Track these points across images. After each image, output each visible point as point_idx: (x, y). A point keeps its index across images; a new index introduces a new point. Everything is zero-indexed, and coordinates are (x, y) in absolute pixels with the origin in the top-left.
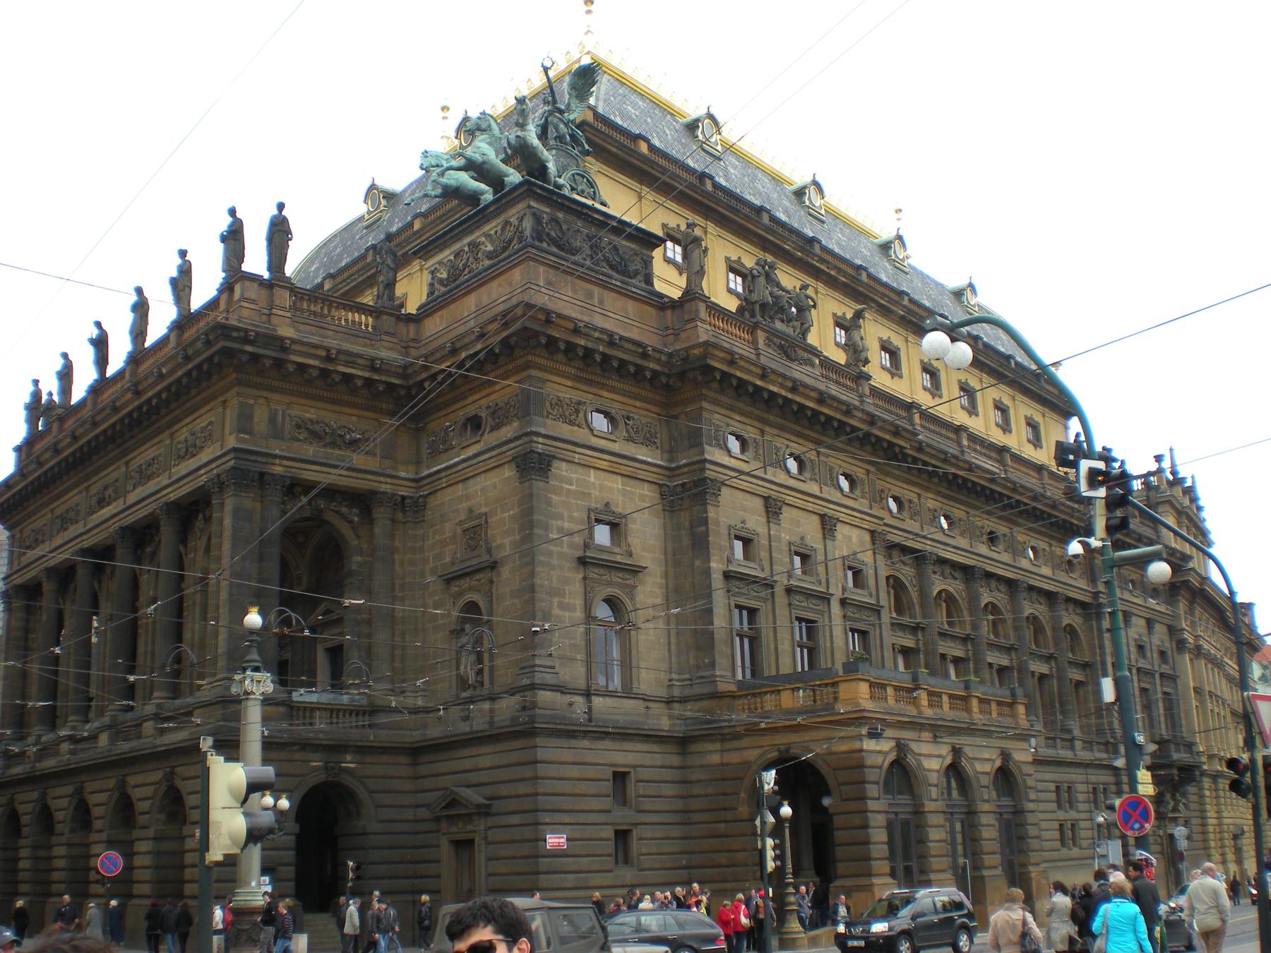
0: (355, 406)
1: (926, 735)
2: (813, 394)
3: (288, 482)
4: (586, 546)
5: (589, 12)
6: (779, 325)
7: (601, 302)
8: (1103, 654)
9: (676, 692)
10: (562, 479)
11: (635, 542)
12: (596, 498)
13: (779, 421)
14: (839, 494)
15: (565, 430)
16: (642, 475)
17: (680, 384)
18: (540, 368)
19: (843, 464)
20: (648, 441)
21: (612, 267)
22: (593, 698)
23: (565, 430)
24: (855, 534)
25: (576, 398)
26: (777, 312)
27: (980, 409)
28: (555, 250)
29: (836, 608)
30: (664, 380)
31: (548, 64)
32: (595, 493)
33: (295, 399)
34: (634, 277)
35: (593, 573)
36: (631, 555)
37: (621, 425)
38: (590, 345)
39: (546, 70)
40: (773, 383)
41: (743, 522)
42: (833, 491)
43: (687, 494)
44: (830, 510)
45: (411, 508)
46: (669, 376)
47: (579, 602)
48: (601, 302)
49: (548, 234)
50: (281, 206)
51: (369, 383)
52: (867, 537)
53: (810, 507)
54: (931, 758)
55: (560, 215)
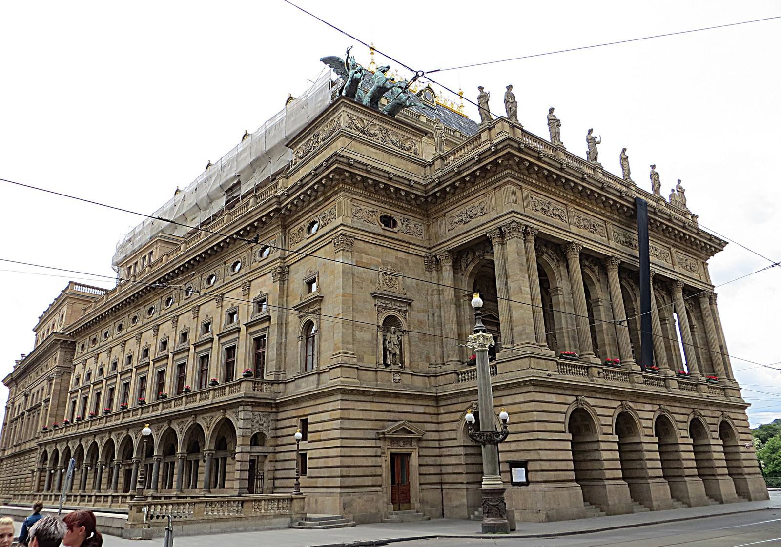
21: (394, 144)
25: (371, 209)
49: (356, 126)
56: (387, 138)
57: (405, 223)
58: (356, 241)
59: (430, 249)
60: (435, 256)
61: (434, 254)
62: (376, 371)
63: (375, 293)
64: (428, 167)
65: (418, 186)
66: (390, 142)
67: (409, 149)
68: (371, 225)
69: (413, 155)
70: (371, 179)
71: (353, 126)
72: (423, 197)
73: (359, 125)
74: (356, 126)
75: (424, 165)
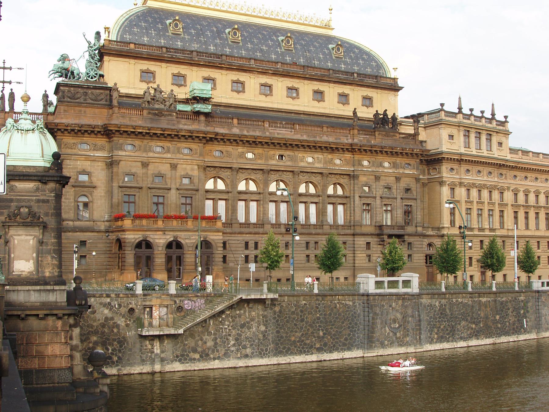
1: (161, 233)
4: (75, 182)
6: (157, 106)
7: (85, 112)
8: (354, 193)
10: (67, 165)
11: (94, 179)
12: (80, 168)
14: (182, 156)
15: (69, 151)
16: (97, 160)
18: (59, 136)
20: (102, 149)
23: (69, 151)
24: (189, 167)
27: (326, 98)
28: (69, 100)
32: (79, 167)
34: (101, 101)
36: (92, 183)
38: (72, 128)
40: (140, 129)
42: (178, 155)
43: (111, 164)
44: (175, 162)
47: (72, 198)
48: (85, 112)
52: (196, 167)
54: (160, 240)
55: (72, 89)
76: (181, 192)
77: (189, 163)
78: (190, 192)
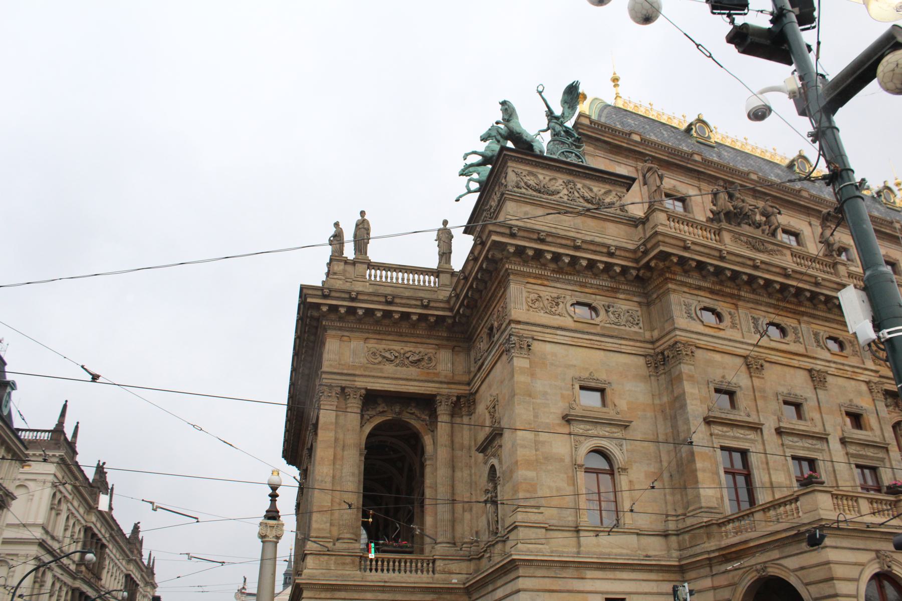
0: (418, 336)
2: (777, 270)
3: (363, 391)
5: (616, 86)
9: (672, 526)
13: (752, 296)
17: (648, 274)
19: (827, 329)
21: (587, 201)
22: (582, 534)
25: (556, 295)
26: (743, 219)
29: (835, 444)
30: (634, 273)
31: (540, 89)
33: (370, 336)
35: (578, 428)
37: (602, 312)
39: (540, 93)
41: (723, 377)
45: (464, 404)
46: (638, 270)
49: (526, 183)
50: (363, 213)
51: (423, 318)
52: (864, 387)
53: (795, 363)
56: (576, 194)
57: (611, 309)
58: (535, 343)
59: (653, 343)
60: (662, 353)
61: (658, 350)
62: (578, 531)
63: (567, 415)
64: (640, 227)
65: (623, 254)
66: (581, 200)
67: (611, 205)
68: (557, 317)
69: (618, 212)
70: (548, 251)
71: (522, 184)
72: (634, 268)
73: (531, 182)
74: (526, 183)
75: (636, 222)
76: (852, 449)
77: (849, 375)
78: (870, 452)
